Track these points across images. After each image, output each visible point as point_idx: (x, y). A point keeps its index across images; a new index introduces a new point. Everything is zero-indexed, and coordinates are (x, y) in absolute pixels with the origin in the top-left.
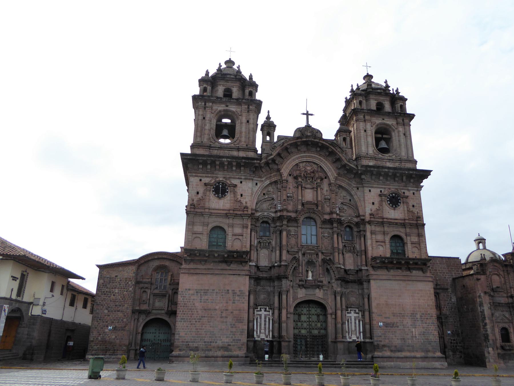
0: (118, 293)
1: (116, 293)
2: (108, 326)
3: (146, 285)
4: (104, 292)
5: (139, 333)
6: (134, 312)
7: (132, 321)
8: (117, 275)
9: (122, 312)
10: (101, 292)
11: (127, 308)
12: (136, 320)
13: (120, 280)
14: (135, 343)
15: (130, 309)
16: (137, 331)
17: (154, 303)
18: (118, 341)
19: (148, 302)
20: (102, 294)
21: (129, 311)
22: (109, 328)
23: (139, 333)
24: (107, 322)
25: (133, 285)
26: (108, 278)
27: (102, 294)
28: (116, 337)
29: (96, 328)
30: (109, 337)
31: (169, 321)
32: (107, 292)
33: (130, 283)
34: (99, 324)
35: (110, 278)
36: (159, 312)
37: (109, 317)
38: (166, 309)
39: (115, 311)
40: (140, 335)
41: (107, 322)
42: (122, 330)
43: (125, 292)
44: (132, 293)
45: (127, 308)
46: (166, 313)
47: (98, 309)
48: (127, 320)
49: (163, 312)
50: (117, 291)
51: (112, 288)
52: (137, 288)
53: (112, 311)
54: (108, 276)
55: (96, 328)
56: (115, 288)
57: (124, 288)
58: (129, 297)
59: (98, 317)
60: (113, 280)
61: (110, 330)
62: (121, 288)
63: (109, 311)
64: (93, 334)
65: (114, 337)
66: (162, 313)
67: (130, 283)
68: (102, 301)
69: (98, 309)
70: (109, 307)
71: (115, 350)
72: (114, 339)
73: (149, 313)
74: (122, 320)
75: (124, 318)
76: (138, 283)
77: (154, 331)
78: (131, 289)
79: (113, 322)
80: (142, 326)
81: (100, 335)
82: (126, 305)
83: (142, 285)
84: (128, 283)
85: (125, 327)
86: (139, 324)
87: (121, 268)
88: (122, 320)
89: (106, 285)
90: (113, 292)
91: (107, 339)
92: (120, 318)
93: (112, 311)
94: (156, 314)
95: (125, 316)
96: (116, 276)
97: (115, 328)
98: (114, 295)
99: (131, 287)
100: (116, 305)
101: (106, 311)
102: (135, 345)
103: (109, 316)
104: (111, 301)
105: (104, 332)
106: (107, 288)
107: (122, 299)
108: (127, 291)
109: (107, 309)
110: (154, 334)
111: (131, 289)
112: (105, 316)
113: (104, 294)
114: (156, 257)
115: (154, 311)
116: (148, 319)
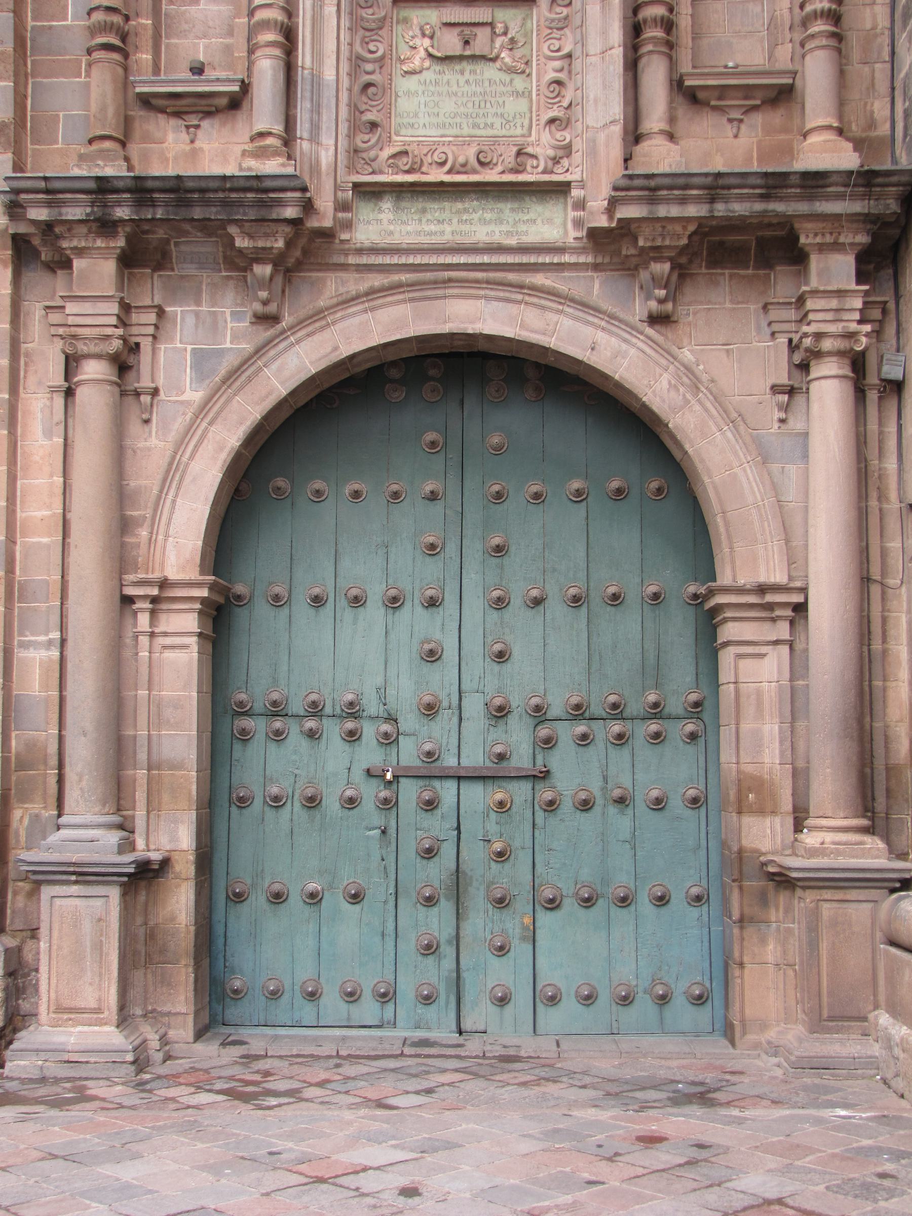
5: (162, 596)
7: (40, 406)
12: (94, 370)
14: (118, 750)
16: (121, 559)
17: (368, 88)
19: (267, 68)
23: (162, 596)
36: (484, 225)
38: (595, 173)
40: (185, 622)
46: (611, 245)
49: (549, 225)
73: (307, 250)
80: (206, 475)
86: (152, 445)
94: (432, 274)
102: (118, 794)
110: (414, 622)
115: (377, 225)
116: (302, 359)
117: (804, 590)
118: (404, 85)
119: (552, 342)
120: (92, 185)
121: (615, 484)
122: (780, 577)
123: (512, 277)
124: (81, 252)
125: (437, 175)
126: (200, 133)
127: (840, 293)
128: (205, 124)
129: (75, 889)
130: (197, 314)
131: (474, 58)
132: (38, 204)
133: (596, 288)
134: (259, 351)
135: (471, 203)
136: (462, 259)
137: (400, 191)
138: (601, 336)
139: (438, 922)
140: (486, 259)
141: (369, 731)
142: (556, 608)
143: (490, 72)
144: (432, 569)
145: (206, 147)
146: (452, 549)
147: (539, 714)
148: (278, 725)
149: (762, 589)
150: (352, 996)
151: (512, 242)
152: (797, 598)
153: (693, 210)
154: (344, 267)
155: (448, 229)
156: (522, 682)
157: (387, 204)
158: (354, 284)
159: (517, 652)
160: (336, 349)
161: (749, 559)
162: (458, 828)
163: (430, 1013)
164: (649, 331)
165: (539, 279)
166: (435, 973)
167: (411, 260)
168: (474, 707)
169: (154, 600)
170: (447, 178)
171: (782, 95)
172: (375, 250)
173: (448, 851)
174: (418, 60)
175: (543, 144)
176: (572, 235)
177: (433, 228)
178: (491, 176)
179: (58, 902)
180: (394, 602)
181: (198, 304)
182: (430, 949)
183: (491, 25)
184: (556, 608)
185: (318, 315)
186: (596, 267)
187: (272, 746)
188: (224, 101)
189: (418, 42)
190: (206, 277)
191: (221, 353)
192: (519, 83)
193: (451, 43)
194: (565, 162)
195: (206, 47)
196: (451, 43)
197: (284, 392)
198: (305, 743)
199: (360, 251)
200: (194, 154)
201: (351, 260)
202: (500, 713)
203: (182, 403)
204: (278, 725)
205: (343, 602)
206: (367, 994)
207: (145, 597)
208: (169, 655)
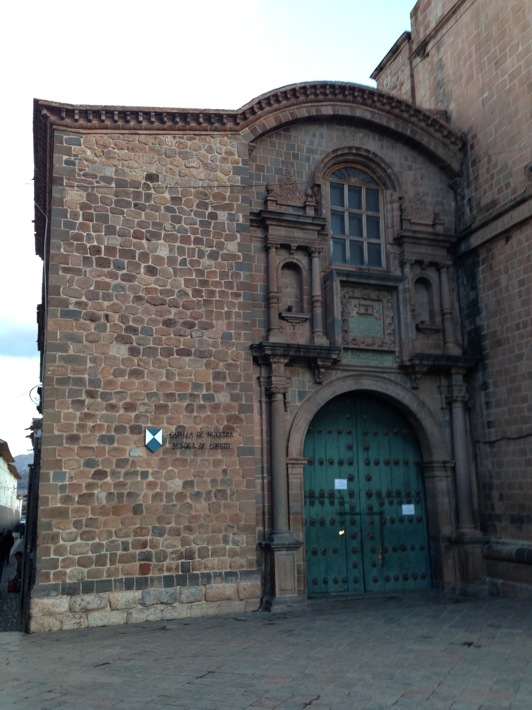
0: (171, 261)
1: (159, 259)
2: (138, 430)
3: (299, 236)
4: (96, 250)
6: (261, 356)
8: (153, 170)
9: (201, 355)
10: (82, 248)
11: (226, 338)
13: (175, 200)
15: (244, 340)
18: (203, 503)
20: (87, 261)
21: (239, 355)
22: (149, 437)
24: (129, 407)
25: (241, 228)
26: (108, 180)
27: (87, 261)
28: (188, 484)
29: (73, 439)
30: (151, 485)
31: (414, 406)
32: (110, 250)
33: (223, 216)
34: (88, 416)
35: (121, 184)
36: (373, 361)
37: (137, 382)
39: (168, 353)
41: (129, 407)
42: (216, 446)
43: (206, 261)
44: (240, 267)
45: (229, 333)
47: (76, 339)
48: (235, 398)
49: (389, 362)
50: (163, 252)
51: (138, 235)
52: (256, 245)
53: (151, 352)
54: (110, 172)
55: (73, 439)
56: (156, 236)
57: (198, 241)
58: (229, 285)
59: (80, 382)
60: (137, 195)
61: (152, 447)
62: (185, 240)
63: (133, 351)
64: (60, 476)
65: (176, 485)
66: (385, 370)
67: (223, 216)
68: (93, 296)
69: (76, 339)
70: (134, 331)
71: (190, 555)
72: (181, 496)
74: (208, 398)
75: (218, 389)
76: (260, 220)
77: (345, 455)
78: (232, 247)
79: (161, 408)
81: (100, 474)
82: (220, 326)
83: (277, 233)
84: (213, 216)
85: (228, 432)
87: (169, 141)
88: (208, 398)
89: (103, 218)
90: (144, 256)
91: (145, 497)
92: (197, 386)
93: (151, 352)
94: (360, 373)
95: (218, 376)
96: (151, 177)
97: (177, 439)
98: (151, 271)
99: (231, 238)
100: (169, 323)
101: (120, 351)
103: (136, 373)
104: (138, 299)
105: (122, 463)
106: (111, 231)
107: (197, 293)
108: (213, 256)
109: (122, 339)
111: (232, 247)
112: (119, 373)
113: (102, 263)
114: (327, 110)
115: (347, 359)
116: (327, 394)
117: (455, 463)
118: (351, 320)
119: (389, 393)
120: (285, 346)
121: (395, 430)
122: (447, 459)
123: (381, 375)
124: (275, 363)
125: (363, 346)
126: (296, 328)
127: (461, 386)
128: (298, 325)
129: (284, 552)
130: (299, 381)
131: (368, 314)
132: (269, 350)
133: (399, 379)
134: (317, 392)
135: (370, 354)
136: (368, 369)
137: (353, 349)
138: (400, 392)
139: (354, 558)
140: (373, 369)
141: (336, 501)
142: (382, 464)
143: (371, 319)
144: (350, 454)
145: (298, 332)
146: (355, 448)
147: (379, 495)
148: (312, 500)
149: (444, 462)
150: (336, 582)
151: (381, 366)
152: (453, 465)
153: (430, 363)
154: (338, 369)
155: (365, 361)
156: (374, 486)
157: (350, 353)
158: (340, 374)
159: (373, 478)
160: (335, 392)
161: (439, 455)
162: (361, 530)
163: (357, 585)
164: (413, 391)
165: (385, 375)
166: (356, 573)
167: (356, 369)
168: (363, 494)
169: (293, 464)
170: (366, 348)
171: (440, 331)
172: (347, 366)
173: (359, 536)
174: (354, 313)
175: (388, 339)
176: (395, 365)
177: (361, 360)
178: (375, 347)
179: (280, 557)
180: (341, 463)
181: (299, 377)
182: (355, 566)
183: (372, 306)
184: (382, 464)
185: (332, 382)
186: (399, 373)
187: (311, 507)
188: (304, 320)
189: (354, 308)
190: (301, 370)
191: (306, 392)
192: (379, 322)
193: (362, 310)
194: (393, 345)
195: (290, 301)
196: (362, 310)
197: (323, 404)
198: (320, 506)
199: (343, 366)
200: (294, 334)
201: (341, 368)
202: (369, 495)
203: (296, 406)
204: (312, 500)
205: (328, 464)
206: (340, 581)
207: (291, 464)
208: (295, 480)
